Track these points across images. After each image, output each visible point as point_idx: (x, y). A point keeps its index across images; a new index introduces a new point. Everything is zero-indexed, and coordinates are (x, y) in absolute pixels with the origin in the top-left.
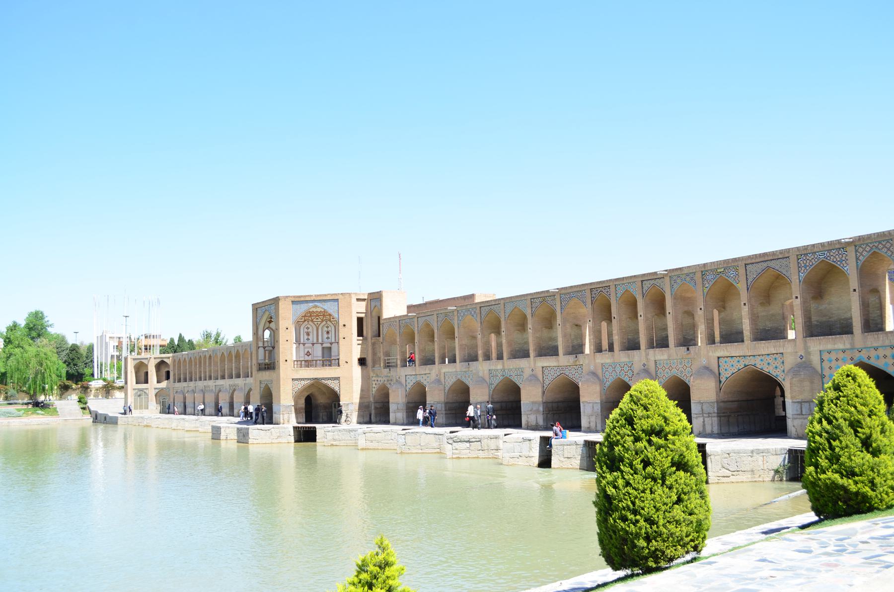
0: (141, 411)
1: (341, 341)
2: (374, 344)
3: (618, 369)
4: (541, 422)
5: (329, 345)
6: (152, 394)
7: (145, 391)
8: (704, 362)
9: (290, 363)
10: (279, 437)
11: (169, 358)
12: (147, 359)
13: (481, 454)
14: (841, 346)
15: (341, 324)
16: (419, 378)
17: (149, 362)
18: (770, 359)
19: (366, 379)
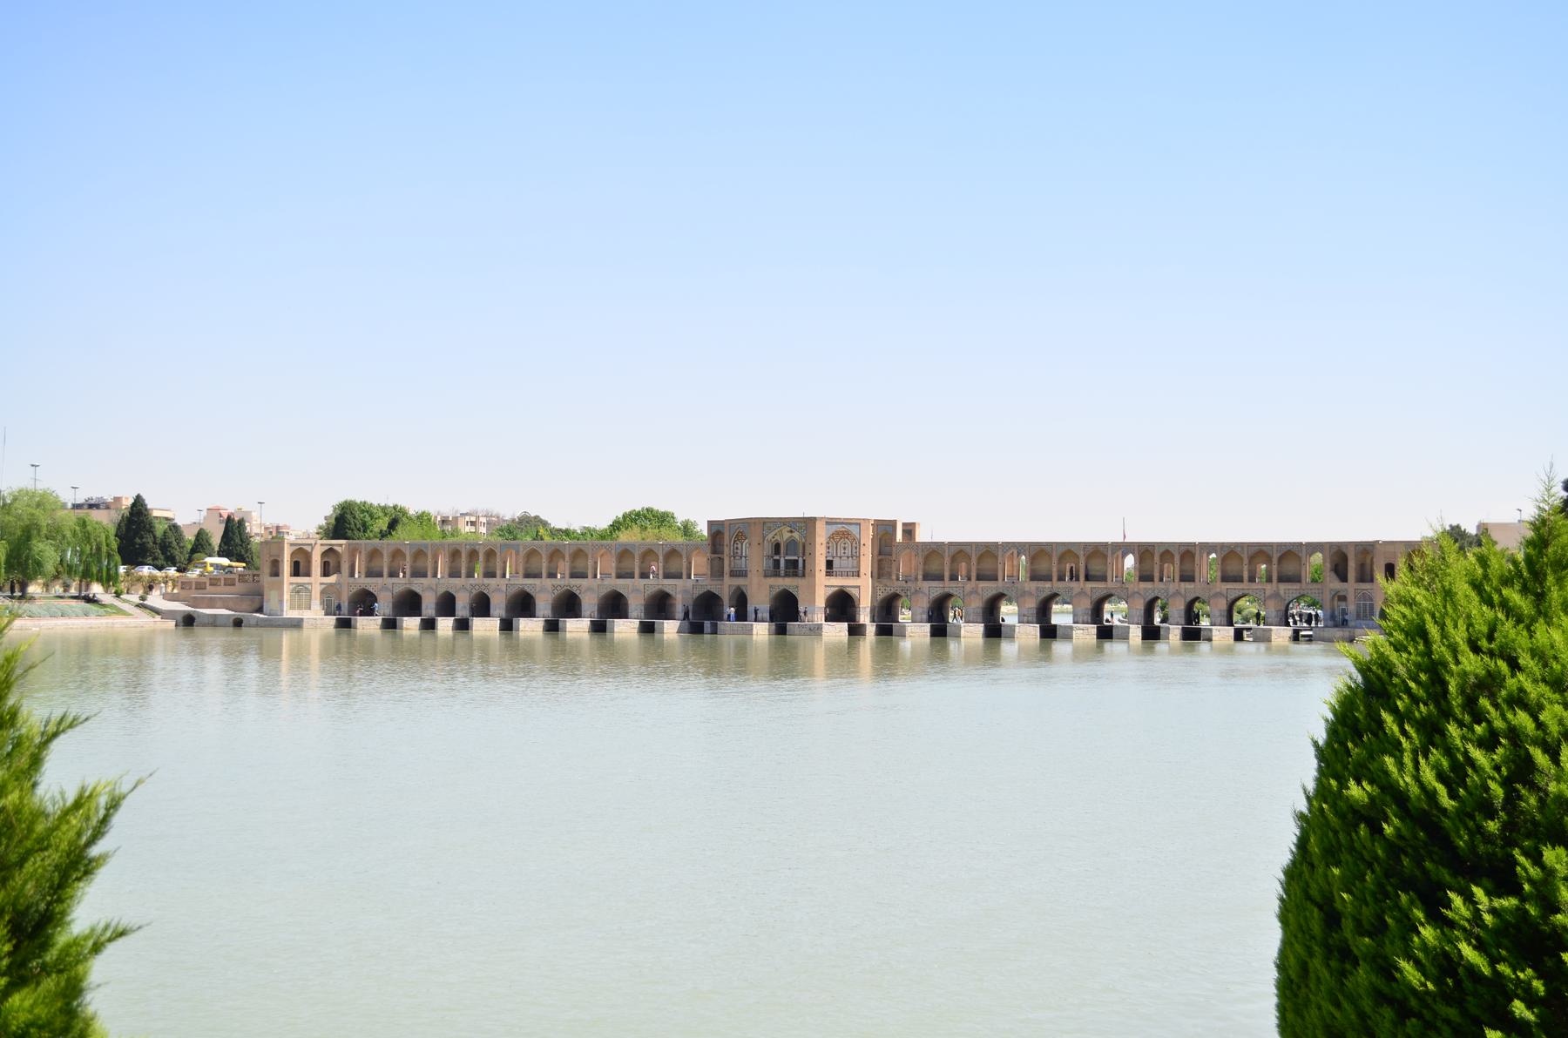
0: (301, 611)
1: (862, 556)
2: (880, 561)
3: (1156, 591)
4: (1090, 621)
5: (831, 559)
6: (316, 591)
7: (307, 586)
8: (1218, 590)
9: (824, 572)
10: (840, 631)
11: (341, 545)
12: (309, 545)
13: (1087, 637)
14: (1295, 587)
15: (862, 543)
16: (947, 590)
17: (312, 549)
18: (1258, 591)
19: (873, 587)
